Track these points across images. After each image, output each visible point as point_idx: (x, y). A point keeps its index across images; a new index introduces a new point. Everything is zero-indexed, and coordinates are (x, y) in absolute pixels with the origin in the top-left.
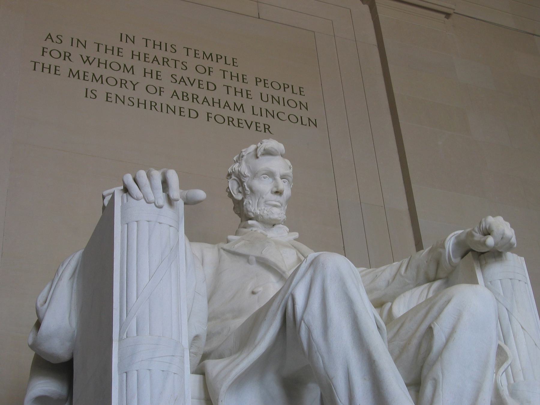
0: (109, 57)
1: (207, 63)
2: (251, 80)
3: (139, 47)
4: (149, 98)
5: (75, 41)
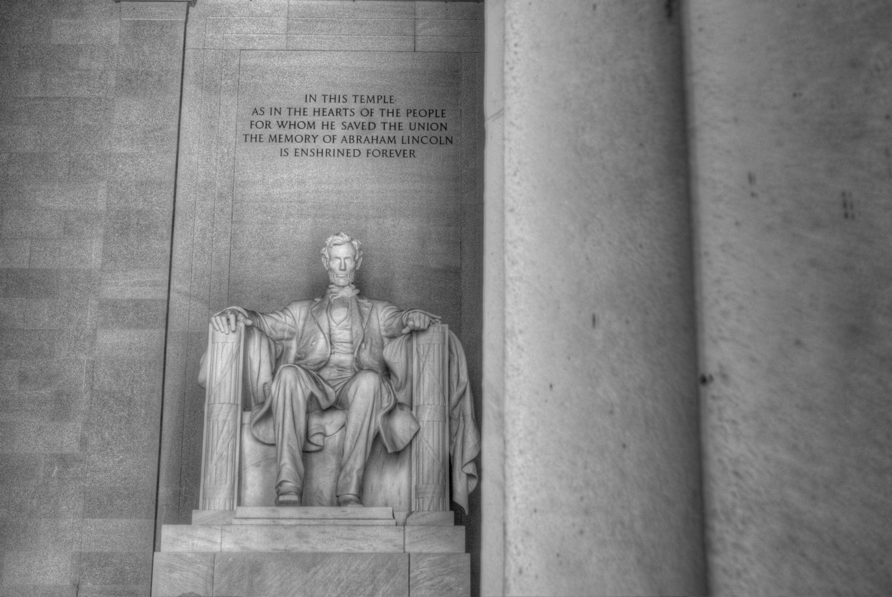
0: (298, 118)
1: (370, 106)
2: (403, 112)
3: (319, 104)
4: (325, 146)
5: (273, 111)
